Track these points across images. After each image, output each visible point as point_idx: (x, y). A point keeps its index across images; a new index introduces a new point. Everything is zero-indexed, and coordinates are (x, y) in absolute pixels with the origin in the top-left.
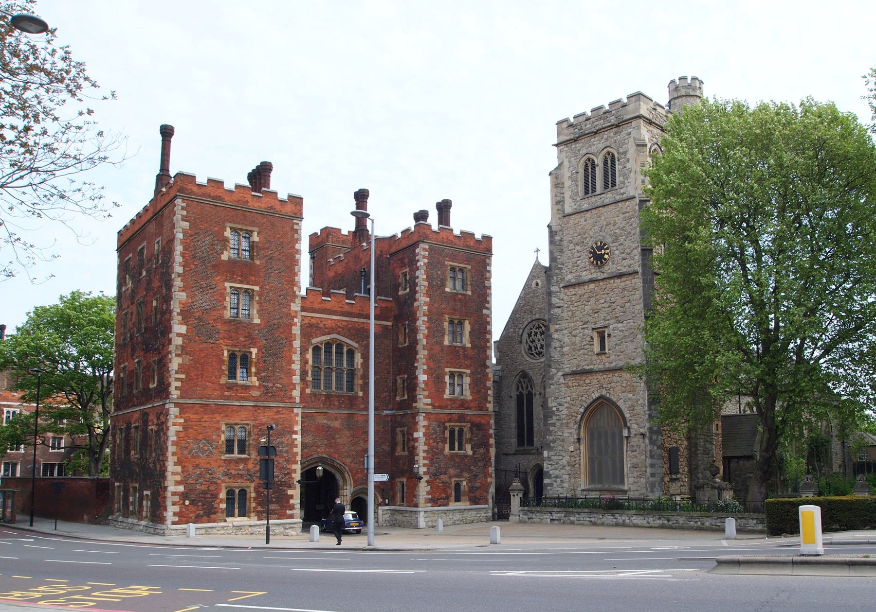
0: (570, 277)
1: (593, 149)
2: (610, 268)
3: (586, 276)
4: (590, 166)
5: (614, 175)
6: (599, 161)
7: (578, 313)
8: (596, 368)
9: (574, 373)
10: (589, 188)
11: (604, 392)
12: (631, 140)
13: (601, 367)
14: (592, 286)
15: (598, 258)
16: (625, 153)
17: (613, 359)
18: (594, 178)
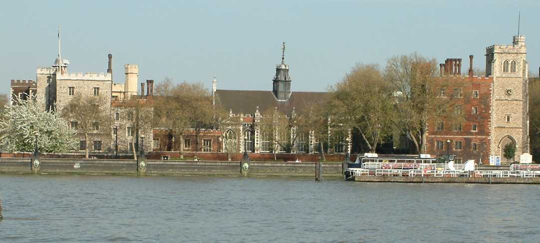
0: (497, 97)
1: (509, 58)
2: (512, 97)
3: (503, 98)
4: (506, 62)
5: (515, 68)
6: (510, 62)
7: (500, 109)
8: (506, 127)
9: (498, 127)
10: (505, 70)
11: (509, 134)
12: (522, 60)
13: (508, 126)
14: (506, 101)
15: (508, 92)
16: (519, 63)
17: (512, 124)
18: (507, 67)
